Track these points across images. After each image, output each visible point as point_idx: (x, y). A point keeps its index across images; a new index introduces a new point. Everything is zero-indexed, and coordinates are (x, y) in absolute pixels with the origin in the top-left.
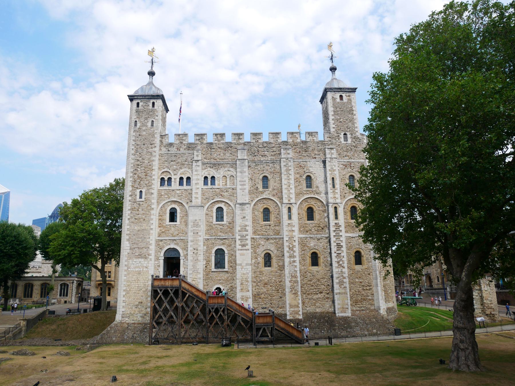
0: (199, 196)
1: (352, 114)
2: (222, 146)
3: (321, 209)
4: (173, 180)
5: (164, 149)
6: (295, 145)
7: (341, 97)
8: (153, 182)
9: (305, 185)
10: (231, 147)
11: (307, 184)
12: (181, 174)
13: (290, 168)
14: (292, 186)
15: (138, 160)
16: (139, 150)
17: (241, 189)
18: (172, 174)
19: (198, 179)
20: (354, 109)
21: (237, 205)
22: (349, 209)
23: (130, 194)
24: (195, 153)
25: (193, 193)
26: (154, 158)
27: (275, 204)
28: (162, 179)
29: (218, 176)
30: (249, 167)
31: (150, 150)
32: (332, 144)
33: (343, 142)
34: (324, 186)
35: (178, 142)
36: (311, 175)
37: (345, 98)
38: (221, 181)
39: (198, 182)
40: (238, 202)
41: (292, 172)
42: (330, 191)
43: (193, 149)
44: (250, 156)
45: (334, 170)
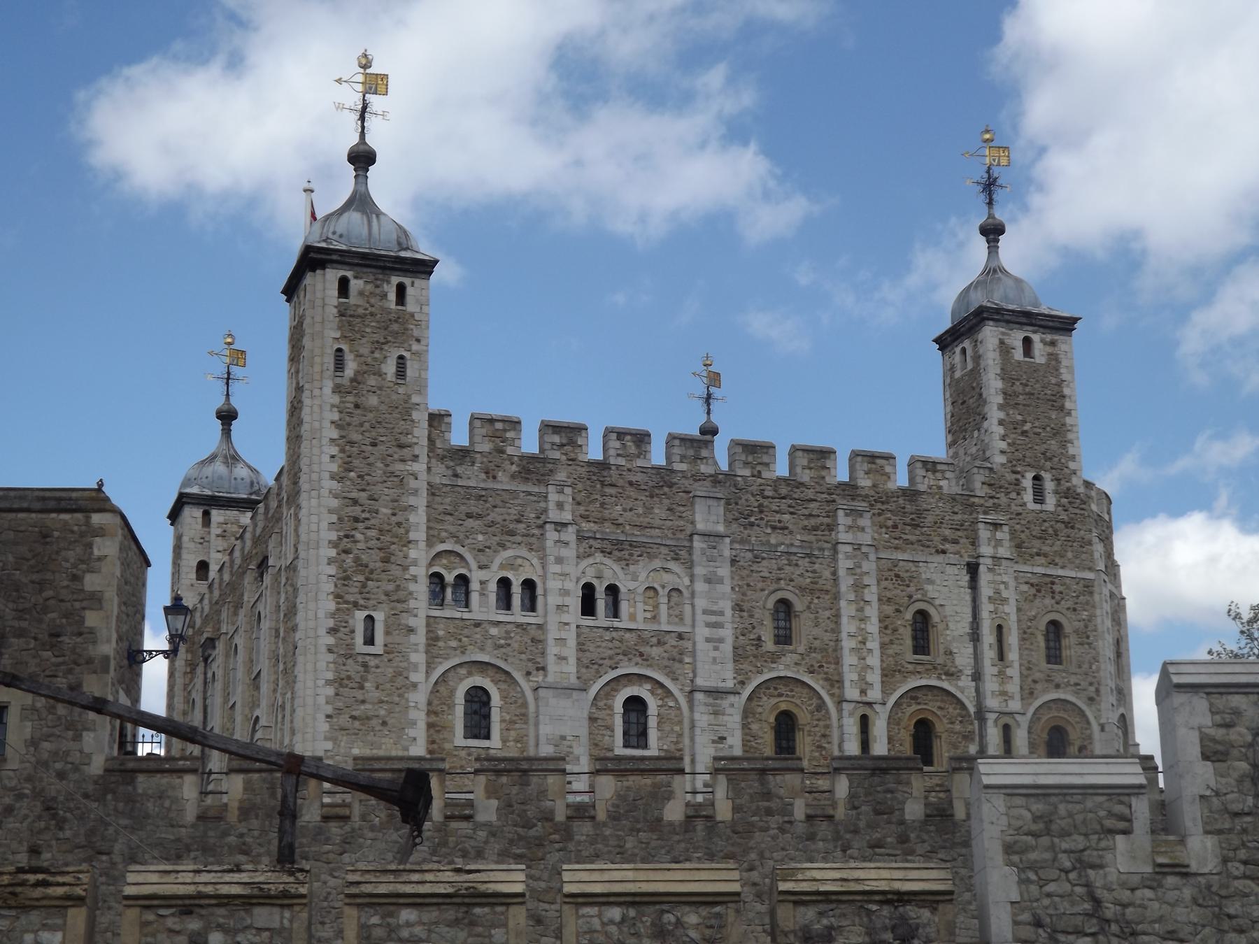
0: (571, 650)
1: (1062, 408)
2: (639, 477)
3: (958, 727)
4: (475, 586)
5: (439, 468)
6: (880, 499)
7: (1027, 342)
8: (412, 587)
9: (909, 642)
10: (671, 485)
11: (915, 638)
12: (502, 567)
13: (866, 580)
14: (874, 645)
15: (355, 502)
16: (356, 462)
17: (708, 640)
18: (474, 565)
19: (565, 592)
20: (1066, 391)
21: (699, 696)
22: (1045, 736)
23: (331, 623)
24: (553, 497)
25: (551, 642)
26: (412, 501)
27: (815, 701)
28: (437, 578)
29: (632, 585)
30: (734, 562)
31: (399, 467)
32: (996, 507)
33: (1031, 506)
34: (971, 650)
35: (486, 447)
36: (932, 611)
37: (1038, 348)
38: (640, 606)
39: (568, 601)
40: (700, 682)
41: (871, 594)
42: (989, 670)
43: (543, 479)
44: (734, 526)
45: (1005, 601)
